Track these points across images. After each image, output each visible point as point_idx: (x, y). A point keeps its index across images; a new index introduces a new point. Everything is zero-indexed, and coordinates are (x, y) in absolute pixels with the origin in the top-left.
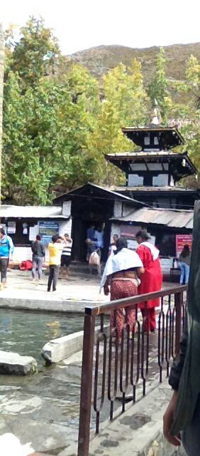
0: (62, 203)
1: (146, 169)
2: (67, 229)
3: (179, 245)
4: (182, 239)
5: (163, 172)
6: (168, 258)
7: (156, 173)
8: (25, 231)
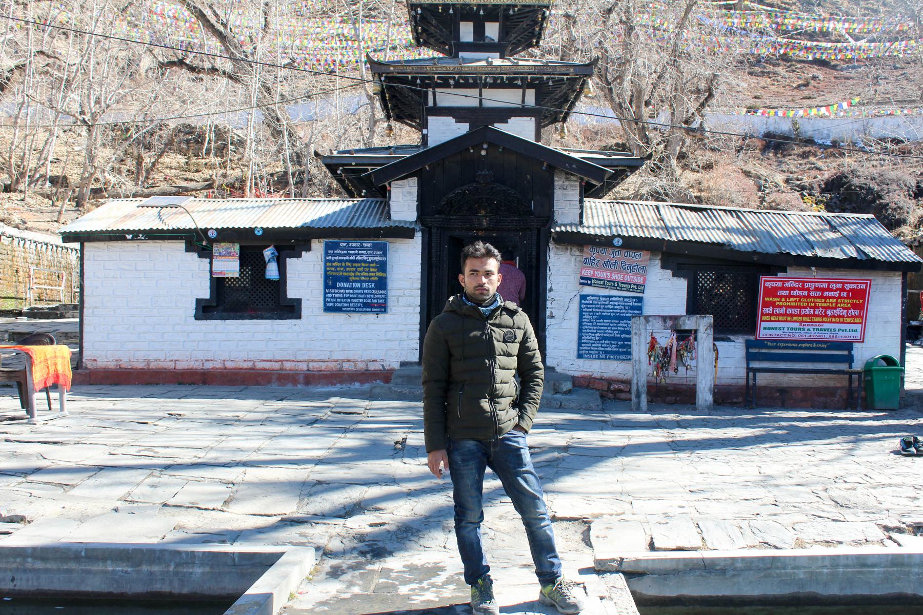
0: (390, 184)
1: (474, 103)
2: (406, 262)
3: (766, 304)
4: (776, 289)
5: (522, 111)
6: (729, 340)
7: (505, 114)
8: (272, 271)
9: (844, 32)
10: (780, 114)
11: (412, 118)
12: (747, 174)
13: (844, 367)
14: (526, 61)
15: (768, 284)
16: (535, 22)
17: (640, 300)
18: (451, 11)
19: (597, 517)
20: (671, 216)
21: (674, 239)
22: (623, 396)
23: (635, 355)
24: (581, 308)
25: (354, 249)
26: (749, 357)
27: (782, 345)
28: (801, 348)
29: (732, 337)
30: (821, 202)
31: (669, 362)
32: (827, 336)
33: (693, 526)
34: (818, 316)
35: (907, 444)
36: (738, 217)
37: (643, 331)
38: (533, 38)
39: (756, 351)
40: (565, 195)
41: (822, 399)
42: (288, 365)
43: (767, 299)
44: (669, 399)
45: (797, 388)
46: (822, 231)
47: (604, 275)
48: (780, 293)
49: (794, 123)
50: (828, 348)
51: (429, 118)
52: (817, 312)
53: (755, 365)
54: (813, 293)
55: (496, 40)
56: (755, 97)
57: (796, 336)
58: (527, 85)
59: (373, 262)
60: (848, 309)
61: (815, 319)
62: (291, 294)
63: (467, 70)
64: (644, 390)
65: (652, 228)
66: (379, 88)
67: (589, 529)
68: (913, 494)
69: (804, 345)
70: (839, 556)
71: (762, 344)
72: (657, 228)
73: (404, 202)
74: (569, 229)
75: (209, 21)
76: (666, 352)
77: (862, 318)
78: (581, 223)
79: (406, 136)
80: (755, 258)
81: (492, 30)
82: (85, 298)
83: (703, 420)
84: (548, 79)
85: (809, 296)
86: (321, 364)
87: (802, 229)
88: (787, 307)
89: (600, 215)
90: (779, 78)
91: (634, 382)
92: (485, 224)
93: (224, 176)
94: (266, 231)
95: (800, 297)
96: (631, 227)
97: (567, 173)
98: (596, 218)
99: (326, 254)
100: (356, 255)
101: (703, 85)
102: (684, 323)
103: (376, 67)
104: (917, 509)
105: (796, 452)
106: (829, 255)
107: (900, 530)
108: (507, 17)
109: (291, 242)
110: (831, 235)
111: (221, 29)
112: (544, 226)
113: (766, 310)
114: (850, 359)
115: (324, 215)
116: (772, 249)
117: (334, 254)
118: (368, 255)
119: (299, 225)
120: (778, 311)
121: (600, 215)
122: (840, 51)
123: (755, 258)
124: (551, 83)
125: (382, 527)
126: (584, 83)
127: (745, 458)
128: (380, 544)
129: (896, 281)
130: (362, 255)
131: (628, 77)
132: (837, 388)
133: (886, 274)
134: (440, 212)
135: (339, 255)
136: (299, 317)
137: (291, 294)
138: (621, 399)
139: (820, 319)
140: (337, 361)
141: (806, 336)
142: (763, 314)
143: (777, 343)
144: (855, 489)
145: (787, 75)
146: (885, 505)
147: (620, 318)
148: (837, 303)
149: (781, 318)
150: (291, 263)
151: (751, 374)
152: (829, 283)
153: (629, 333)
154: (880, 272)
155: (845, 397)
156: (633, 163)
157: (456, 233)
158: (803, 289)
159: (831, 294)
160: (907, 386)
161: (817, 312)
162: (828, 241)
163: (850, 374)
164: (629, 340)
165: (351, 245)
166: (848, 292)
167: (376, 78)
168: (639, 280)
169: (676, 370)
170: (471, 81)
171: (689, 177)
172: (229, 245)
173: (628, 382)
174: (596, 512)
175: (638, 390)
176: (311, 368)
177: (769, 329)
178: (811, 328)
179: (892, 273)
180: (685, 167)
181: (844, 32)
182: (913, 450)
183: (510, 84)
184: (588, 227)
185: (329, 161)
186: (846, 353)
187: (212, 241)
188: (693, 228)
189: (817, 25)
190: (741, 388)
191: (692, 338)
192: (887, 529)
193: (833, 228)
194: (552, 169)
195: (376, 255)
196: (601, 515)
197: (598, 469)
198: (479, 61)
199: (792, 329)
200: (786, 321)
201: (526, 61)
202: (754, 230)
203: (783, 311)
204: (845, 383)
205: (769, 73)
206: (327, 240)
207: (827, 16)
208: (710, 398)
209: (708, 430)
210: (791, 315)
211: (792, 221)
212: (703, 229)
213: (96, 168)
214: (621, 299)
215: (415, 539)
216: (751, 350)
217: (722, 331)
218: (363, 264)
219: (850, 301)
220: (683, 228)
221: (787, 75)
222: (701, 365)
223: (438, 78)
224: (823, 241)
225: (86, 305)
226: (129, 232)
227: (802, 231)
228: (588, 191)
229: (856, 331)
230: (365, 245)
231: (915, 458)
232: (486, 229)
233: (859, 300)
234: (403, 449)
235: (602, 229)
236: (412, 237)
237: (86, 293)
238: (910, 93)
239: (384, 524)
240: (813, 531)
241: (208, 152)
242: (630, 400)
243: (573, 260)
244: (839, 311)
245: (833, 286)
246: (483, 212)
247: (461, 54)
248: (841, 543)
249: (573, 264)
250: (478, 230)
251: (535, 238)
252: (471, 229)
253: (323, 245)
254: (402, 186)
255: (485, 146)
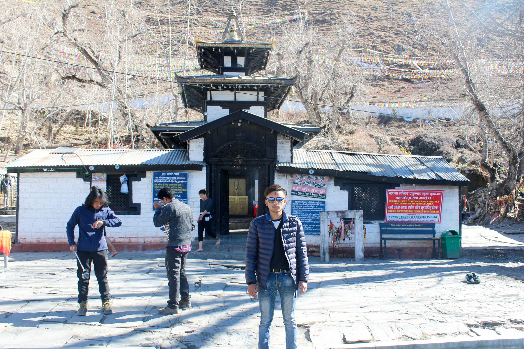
0: (189, 141)
3: (390, 204)
6: (371, 223)
8: (124, 189)
9: (416, 65)
10: (387, 105)
11: (198, 107)
12: (372, 136)
13: (431, 236)
14: (260, 76)
15: (391, 193)
16: (264, 57)
17: (324, 202)
18: (220, 51)
19: (312, 324)
20: (339, 158)
21: (341, 170)
22: (315, 254)
23: (322, 232)
24: (292, 207)
25: (169, 176)
26: (382, 232)
27: (399, 225)
28: (408, 227)
29: (372, 222)
30: (409, 150)
31: (340, 236)
32: (421, 220)
33: (366, 328)
34: (417, 210)
35: (469, 277)
36: (373, 158)
37: (326, 219)
38: (262, 65)
39: (385, 228)
40: (283, 147)
41: (420, 254)
42: (133, 240)
43: (390, 201)
44: (340, 255)
45: (406, 248)
46: (417, 165)
47: (304, 189)
48: (397, 198)
49: (394, 110)
50: (422, 227)
51: (208, 106)
52: (416, 208)
53: (385, 236)
54: (414, 198)
55: (243, 66)
56: (374, 97)
57: (406, 220)
58: (260, 89)
59: (180, 183)
60: (432, 206)
61: (415, 211)
62: (135, 201)
63: (228, 81)
64: (327, 251)
65: (329, 164)
66: (181, 91)
67: (309, 331)
68: (478, 305)
69: (410, 225)
70: (449, 343)
71: (388, 225)
72: (332, 164)
73: (196, 151)
74: (285, 165)
75: (89, 55)
76: (338, 230)
77: (439, 210)
78: (292, 162)
79: (195, 116)
80: (384, 180)
81: (241, 61)
82: (20, 204)
83: (360, 266)
84: (271, 86)
85: (412, 200)
86: (152, 239)
87: (407, 164)
88: (401, 205)
89: (301, 157)
90: (385, 87)
91: (322, 247)
92: (240, 162)
93: (96, 137)
94: (121, 167)
95: (407, 200)
96: (318, 163)
97: (284, 135)
98: (299, 159)
99: (154, 179)
100: (171, 180)
101: (348, 91)
102: (348, 215)
103: (179, 79)
104: (482, 313)
105: (412, 282)
106: (422, 178)
107: (476, 326)
108: (249, 54)
109: (135, 173)
110: (421, 167)
111: (96, 60)
112: (272, 163)
113: (390, 207)
114: (433, 232)
115: (153, 158)
116: (392, 175)
117: (159, 179)
118: (177, 180)
119: (139, 163)
120: (396, 207)
121: (301, 157)
122: (415, 74)
123: (384, 180)
124: (272, 88)
125: (192, 333)
126: (290, 88)
127: (387, 287)
128: (192, 344)
129: (456, 191)
130: (174, 180)
131: (310, 86)
132: (428, 247)
133: (451, 187)
134: (216, 157)
135: (162, 180)
136: (139, 213)
137: (135, 201)
138: (314, 256)
139: (418, 211)
140: (160, 237)
141: (411, 221)
142: (388, 209)
143: (396, 224)
144: (447, 303)
145: (389, 86)
146: (465, 312)
147: (313, 212)
148: (426, 203)
149: (398, 211)
150: (135, 184)
151: (383, 241)
152: (422, 192)
153: (318, 220)
154: (448, 186)
155: (431, 252)
156: (316, 131)
157: (225, 168)
158: (409, 196)
159: (423, 198)
160: (463, 246)
161: (416, 208)
162: (420, 170)
163: (434, 240)
164: (319, 224)
165: (168, 174)
166: (432, 197)
167: (180, 85)
168: (323, 192)
169: (344, 239)
170: (230, 87)
171: (342, 138)
172: (101, 174)
173: (318, 247)
174: (311, 321)
175: (324, 251)
176: (146, 241)
177: (392, 217)
178: (413, 216)
179: (453, 187)
180: (340, 132)
181: (416, 65)
182: (473, 280)
183: (251, 89)
184: (295, 164)
185: (154, 129)
186: (431, 229)
187: (91, 172)
188: (350, 164)
189: (404, 61)
190: (376, 249)
191: (352, 223)
192: (469, 325)
193: (422, 164)
194: (276, 133)
195: (182, 180)
196: (314, 323)
197: (308, 296)
198: (234, 77)
199: (403, 217)
200: (400, 213)
201: (260, 76)
202: (382, 164)
203: (398, 207)
204: (432, 245)
205: (380, 85)
206: (155, 171)
207: (408, 57)
208: (362, 254)
209: (363, 272)
210: (403, 209)
211: (401, 160)
212: (356, 164)
213: (26, 133)
214: (314, 202)
215: (212, 340)
216: (383, 229)
217: (368, 218)
218: (174, 185)
219: (433, 202)
220: (345, 164)
221: (389, 86)
222: (357, 237)
223: (213, 85)
224: (418, 170)
225: (20, 208)
226: (45, 167)
227: (406, 165)
228: (294, 144)
229: (436, 217)
230: (175, 174)
231: (474, 285)
232: (241, 165)
233: (438, 200)
234: (200, 286)
235: (303, 165)
236: (201, 169)
237: (20, 201)
238: (450, 95)
239: (193, 331)
240: (431, 328)
241: (88, 125)
242: (320, 256)
243: (287, 181)
244: (427, 207)
245: (424, 194)
246: (239, 156)
247: (224, 73)
248: (446, 334)
249: (287, 184)
250: (237, 166)
251: (267, 170)
252: (233, 165)
253: (152, 174)
254: (196, 142)
255: (240, 121)
